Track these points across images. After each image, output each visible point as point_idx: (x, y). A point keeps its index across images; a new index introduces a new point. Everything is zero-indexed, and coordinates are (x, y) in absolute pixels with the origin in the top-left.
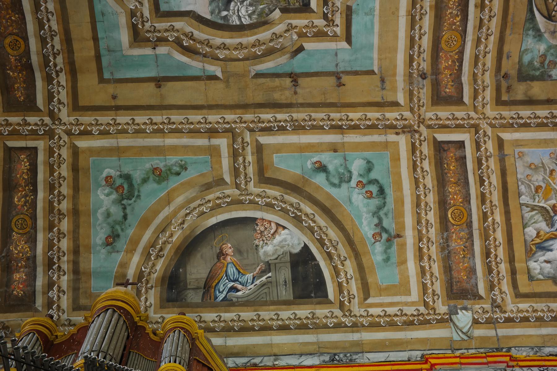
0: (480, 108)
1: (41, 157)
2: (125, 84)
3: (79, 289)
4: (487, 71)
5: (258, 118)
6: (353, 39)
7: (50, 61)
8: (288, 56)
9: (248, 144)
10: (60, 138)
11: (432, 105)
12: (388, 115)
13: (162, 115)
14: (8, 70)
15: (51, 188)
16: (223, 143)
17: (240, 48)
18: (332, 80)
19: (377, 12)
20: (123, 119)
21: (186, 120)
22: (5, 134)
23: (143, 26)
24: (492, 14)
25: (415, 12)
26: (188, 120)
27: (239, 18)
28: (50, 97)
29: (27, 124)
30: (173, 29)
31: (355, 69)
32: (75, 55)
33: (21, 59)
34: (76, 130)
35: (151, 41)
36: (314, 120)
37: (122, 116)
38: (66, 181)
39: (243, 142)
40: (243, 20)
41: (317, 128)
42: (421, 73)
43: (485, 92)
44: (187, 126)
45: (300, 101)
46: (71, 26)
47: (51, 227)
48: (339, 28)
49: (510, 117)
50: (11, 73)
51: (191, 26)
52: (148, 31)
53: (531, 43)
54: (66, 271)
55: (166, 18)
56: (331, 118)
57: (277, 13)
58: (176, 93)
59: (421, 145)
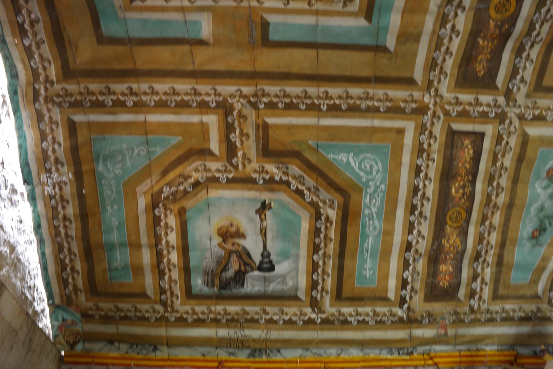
1: (487, 144)
3: (500, 279)
10: (511, 123)
14: (480, 37)
15: (491, 179)
28: (514, 72)
29: (478, 103)
34: (529, 114)
38: (507, 173)
47: (484, 219)
54: (490, 263)
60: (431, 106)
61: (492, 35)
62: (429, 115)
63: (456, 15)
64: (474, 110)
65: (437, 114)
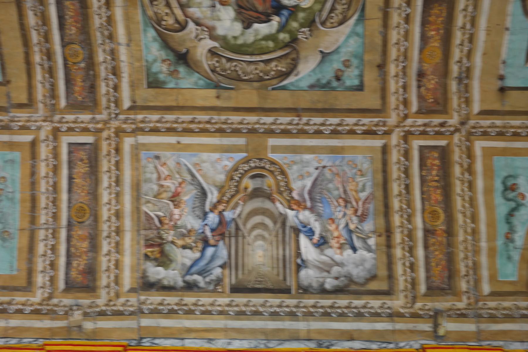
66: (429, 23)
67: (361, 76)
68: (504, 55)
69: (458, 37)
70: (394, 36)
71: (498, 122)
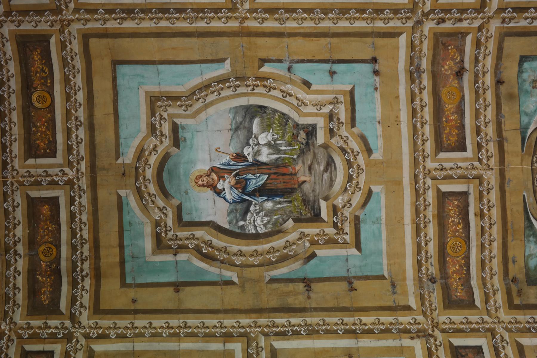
0: (493, 312)
2: (145, 288)
4: (495, 275)
5: (272, 323)
6: (363, 246)
7: (78, 267)
8: (301, 262)
9: (263, 349)
10: (78, 341)
11: (444, 309)
12: (401, 319)
13: (179, 319)
14: (38, 275)
16: (237, 347)
17: (255, 255)
18: (344, 285)
19: (383, 221)
20: (141, 322)
21: (202, 324)
22: (25, 338)
23: (166, 234)
24: (492, 222)
25: (419, 221)
26: (204, 324)
27: (255, 227)
28: (73, 300)
30: (193, 238)
31: (365, 274)
32: (102, 261)
33: (51, 265)
34: (94, 333)
35: (172, 248)
36: (328, 325)
37: (140, 320)
39: (257, 347)
40: (258, 229)
41: (331, 333)
42: (430, 277)
43: (496, 296)
44: (203, 330)
45: (314, 305)
46: (101, 235)
48: (348, 236)
49: (525, 321)
50: (40, 278)
51: (211, 234)
52: (170, 239)
53: (534, 249)
55: (187, 228)
56: (344, 322)
57: (290, 223)
58: (194, 298)
59: (437, 350)
60: (7, 332)
61: (46, 272)
62: (5, 340)
63: (16, 261)
64: (43, 332)
65: (11, 338)
66: (457, 128)
67: (520, 71)
68: (377, 95)
69: (427, 114)
70: (490, 113)
71: (380, 24)
